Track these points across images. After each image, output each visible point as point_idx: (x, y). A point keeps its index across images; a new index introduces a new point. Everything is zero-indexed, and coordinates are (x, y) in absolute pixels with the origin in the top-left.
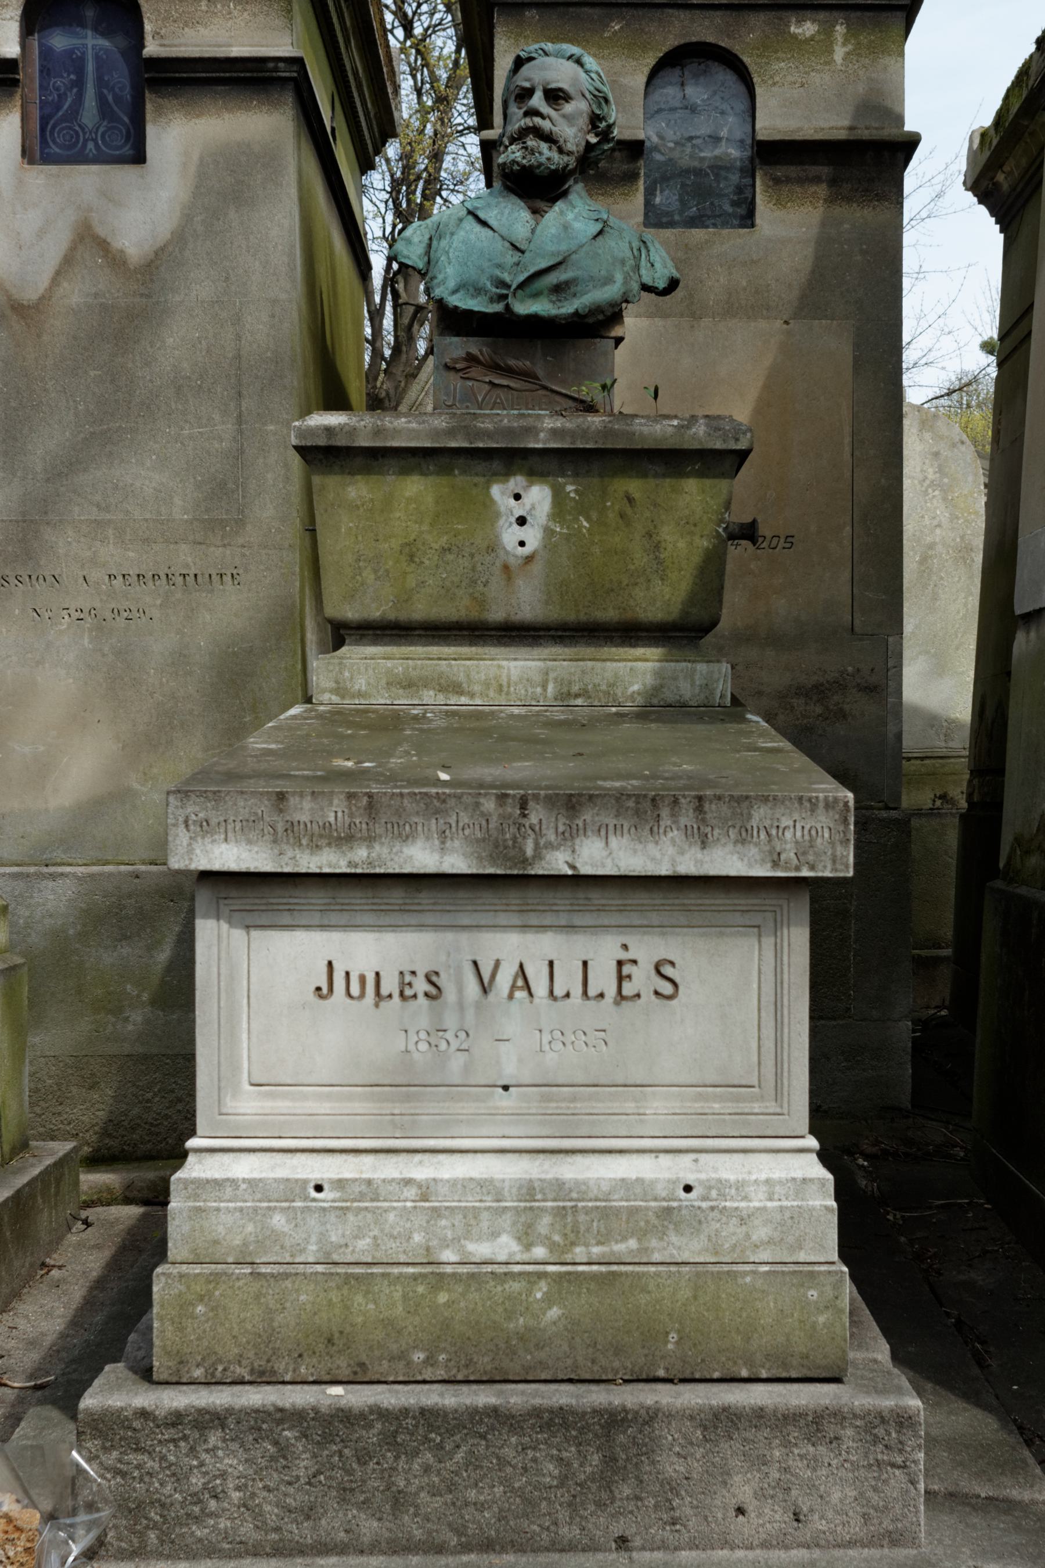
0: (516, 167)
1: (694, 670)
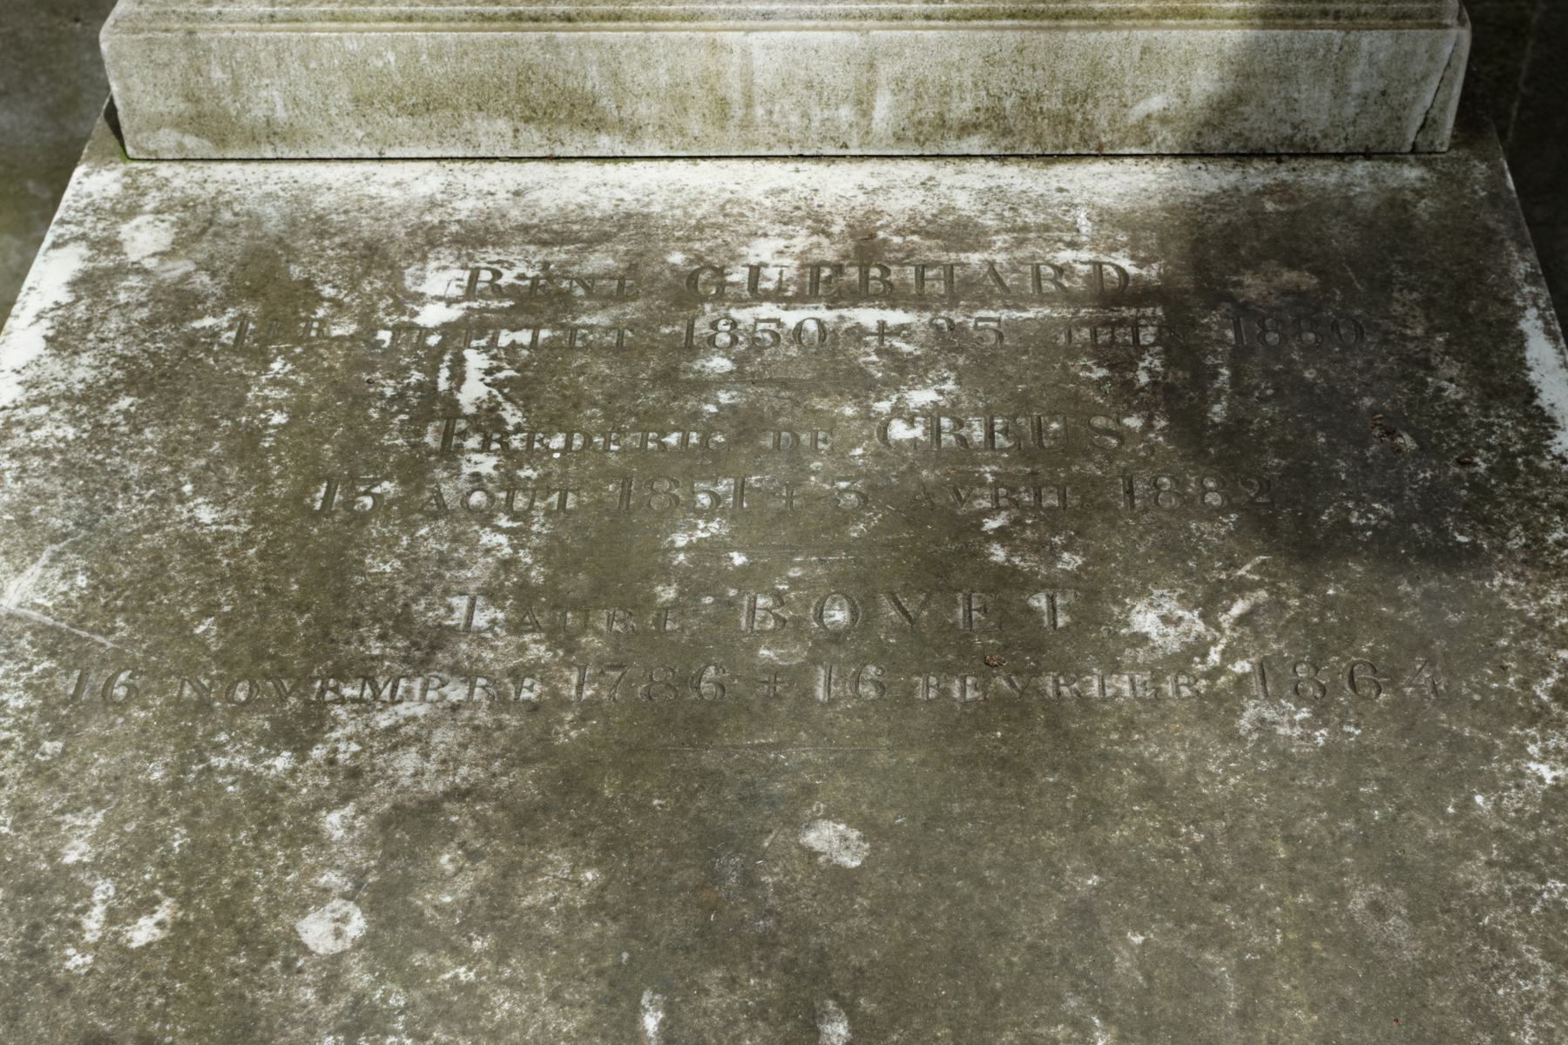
1: (1349, 52)
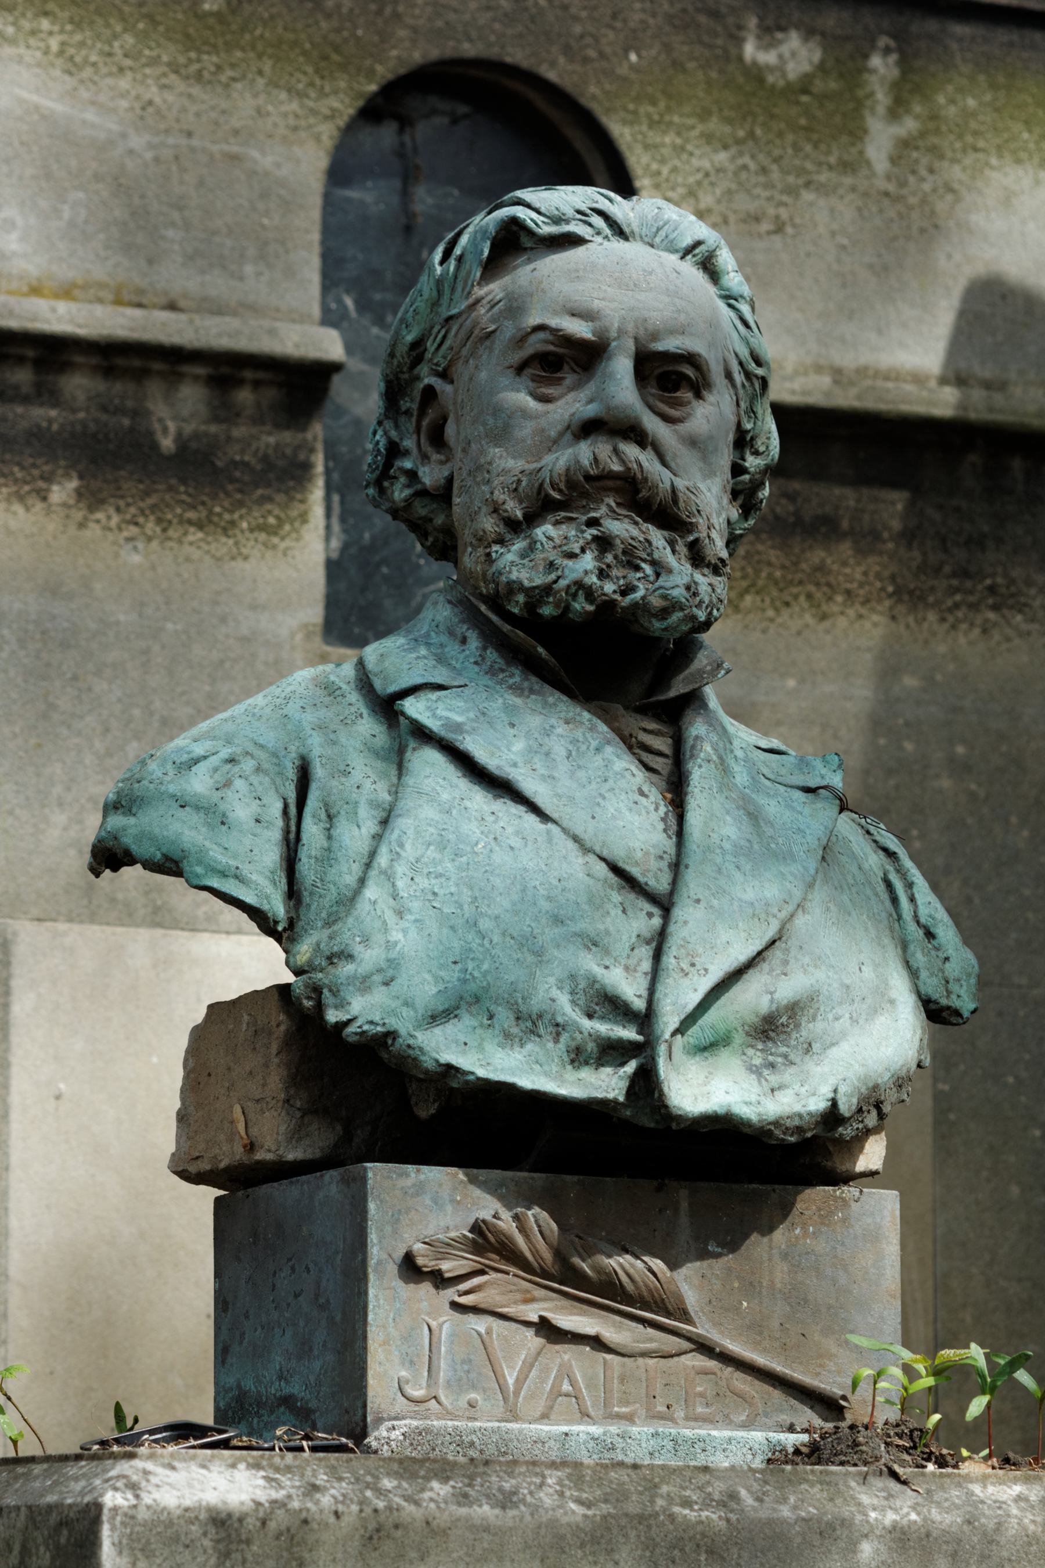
0: (581, 605)
